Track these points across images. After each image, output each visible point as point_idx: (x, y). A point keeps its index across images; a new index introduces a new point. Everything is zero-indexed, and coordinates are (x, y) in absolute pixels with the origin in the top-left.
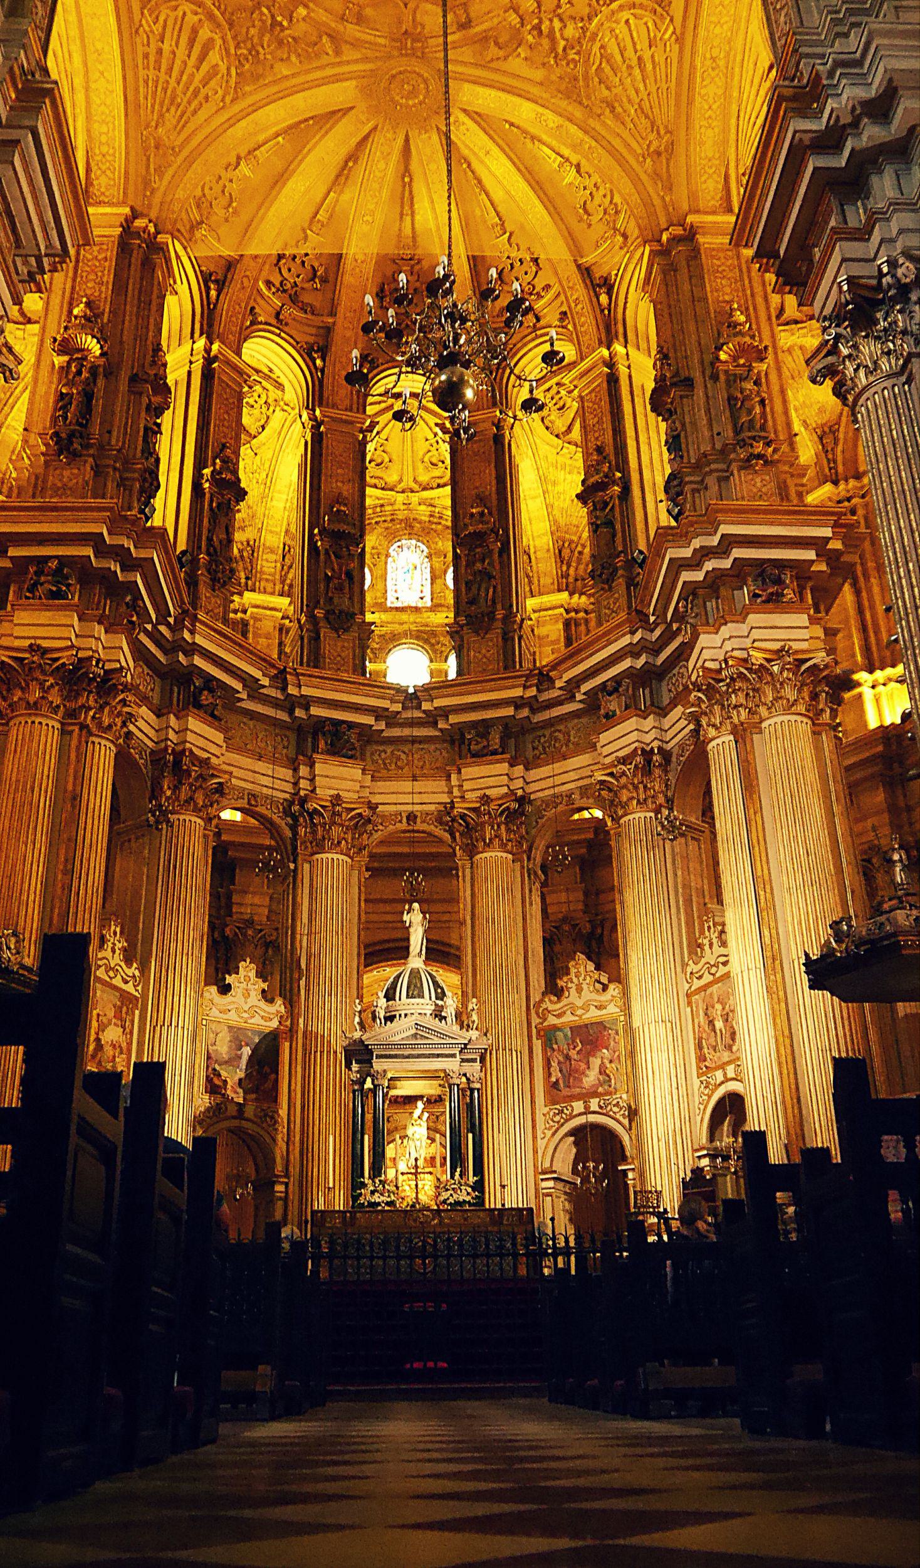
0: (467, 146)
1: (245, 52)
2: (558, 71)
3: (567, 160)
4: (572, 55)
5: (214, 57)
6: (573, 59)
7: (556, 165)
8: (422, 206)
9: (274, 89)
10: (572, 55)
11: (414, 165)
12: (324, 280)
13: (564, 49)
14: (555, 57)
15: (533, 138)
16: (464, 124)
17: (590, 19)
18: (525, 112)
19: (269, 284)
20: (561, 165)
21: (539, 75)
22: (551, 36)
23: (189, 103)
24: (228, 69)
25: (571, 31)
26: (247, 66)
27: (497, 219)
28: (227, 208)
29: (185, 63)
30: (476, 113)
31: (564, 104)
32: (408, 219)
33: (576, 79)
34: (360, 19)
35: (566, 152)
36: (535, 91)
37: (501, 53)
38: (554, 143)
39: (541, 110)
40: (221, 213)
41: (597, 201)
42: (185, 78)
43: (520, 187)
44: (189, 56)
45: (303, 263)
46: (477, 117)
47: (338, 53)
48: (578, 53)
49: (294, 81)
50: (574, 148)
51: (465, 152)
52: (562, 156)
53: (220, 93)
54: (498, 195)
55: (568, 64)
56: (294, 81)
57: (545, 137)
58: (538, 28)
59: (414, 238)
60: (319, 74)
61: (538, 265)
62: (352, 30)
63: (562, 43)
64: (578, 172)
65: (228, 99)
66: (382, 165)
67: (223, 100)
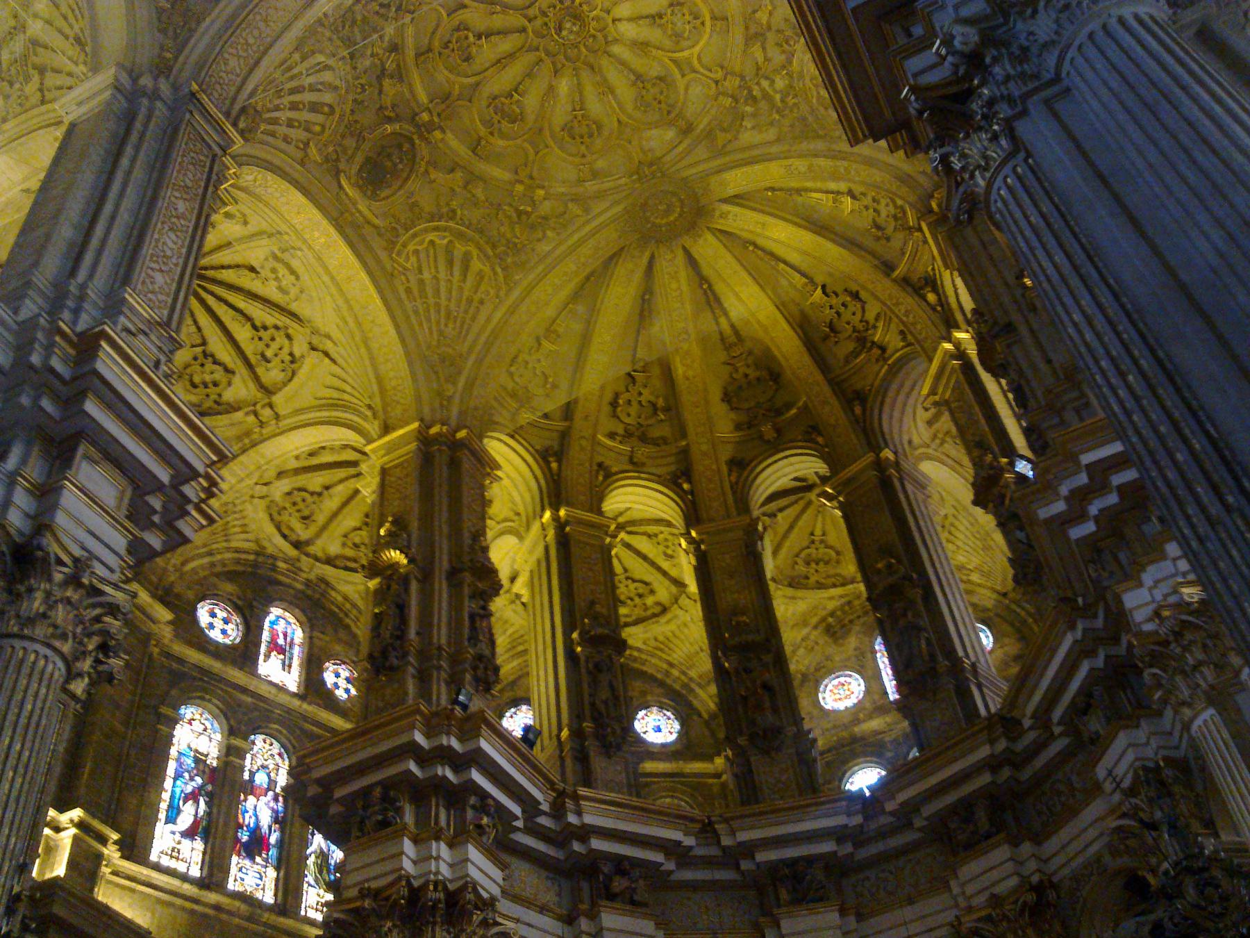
0: (742, 230)
1: (503, 248)
2: (787, 122)
3: (838, 193)
4: (791, 101)
5: (476, 265)
6: (795, 104)
7: (830, 203)
8: (730, 302)
9: (540, 268)
10: (791, 101)
11: (706, 271)
12: (667, 409)
13: (782, 101)
14: (778, 112)
15: (799, 191)
16: (729, 212)
17: (790, 63)
18: (773, 173)
19: (612, 435)
20: (835, 201)
21: (771, 134)
22: (766, 96)
23: (466, 312)
24: (493, 269)
25: (780, 83)
26: (509, 260)
27: (804, 280)
28: (544, 386)
29: (461, 289)
30: (736, 196)
31: (804, 146)
32: (723, 320)
33: (804, 119)
34: (595, 175)
35: (833, 186)
36: (774, 149)
37: (729, 136)
38: (819, 185)
39: (786, 162)
40: (540, 392)
41: (884, 214)
42: (454, 293)
43: (807, 239)
44: (452, 275)
45: (640, 402)
46: (737, 199)
47: (587, 210)
48: (795, 96)
49: (558, 252)
50: (835, 177)
51: (745, 235)
52: (832, 192)
53: (492, 292)
54: (794, 258)
55: (791, 111)
56: (558, 252)
57: (809, 184)
58: (753, 99)
59: (736, 332)
60: (576, 237)
61: (860, 300)
62: (591, 187)
63: (778, 97)
64: (854, 197)
65: (502, 293)
66: (674, 286)
67: (497, 297)
